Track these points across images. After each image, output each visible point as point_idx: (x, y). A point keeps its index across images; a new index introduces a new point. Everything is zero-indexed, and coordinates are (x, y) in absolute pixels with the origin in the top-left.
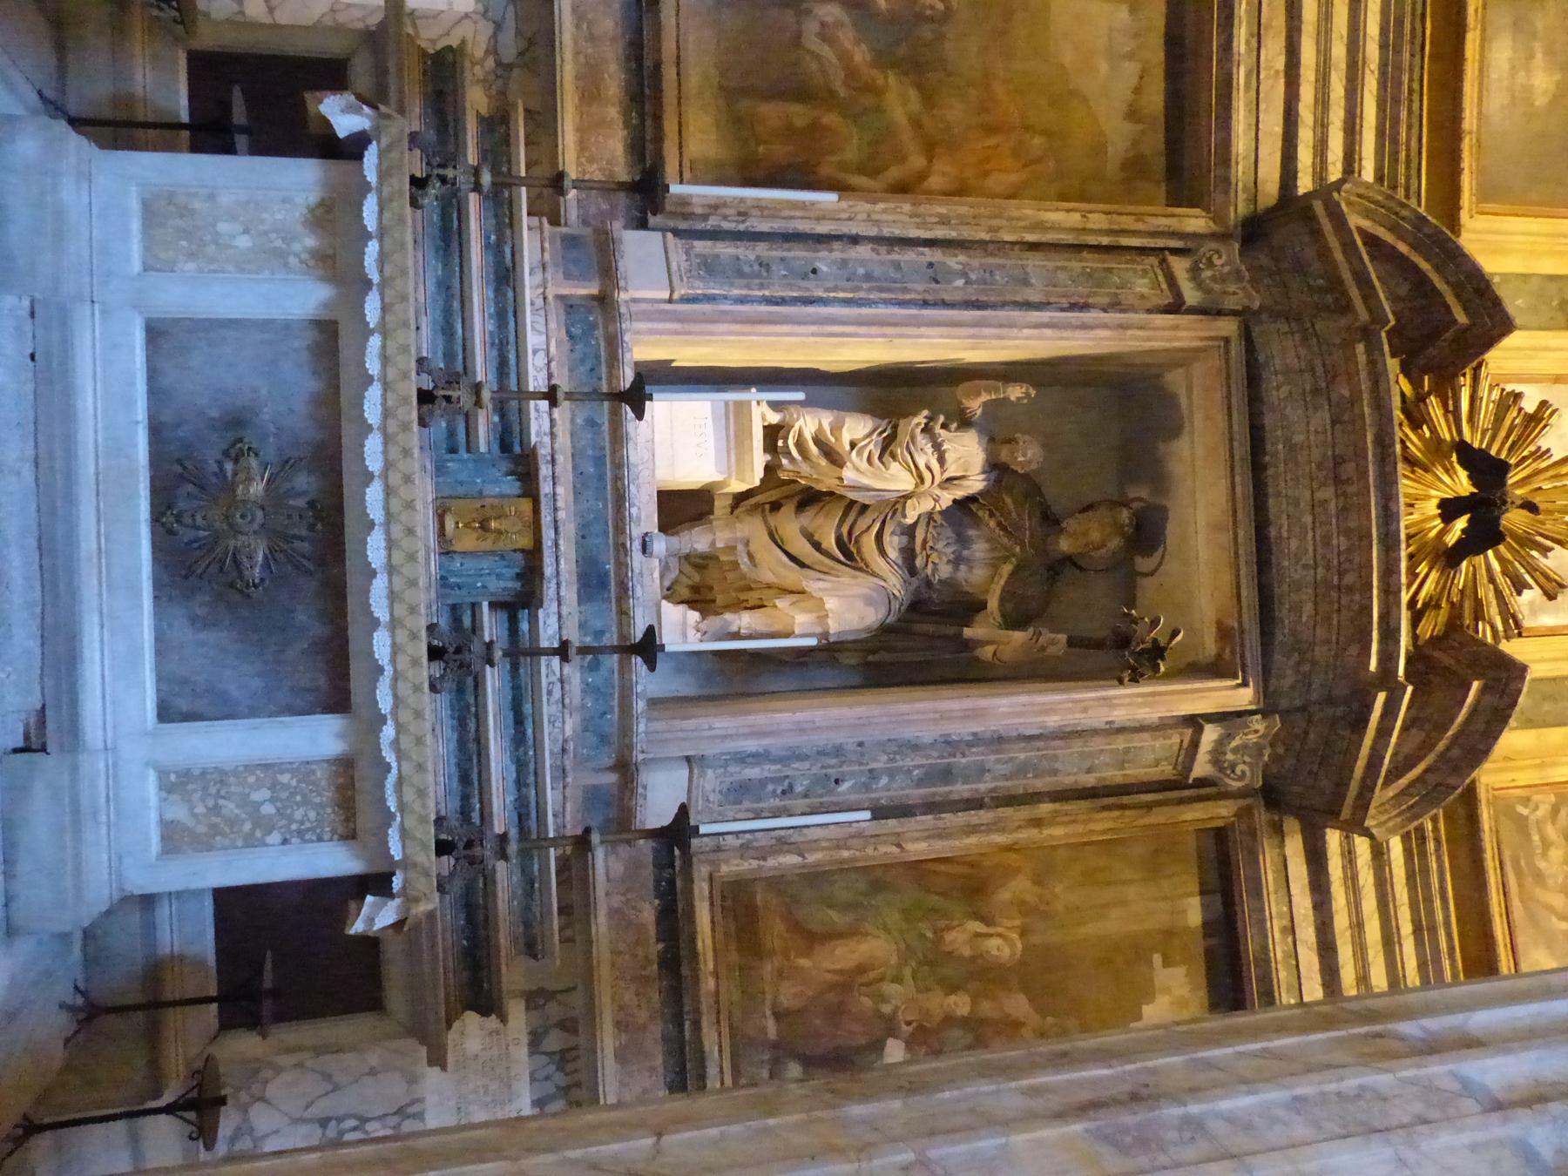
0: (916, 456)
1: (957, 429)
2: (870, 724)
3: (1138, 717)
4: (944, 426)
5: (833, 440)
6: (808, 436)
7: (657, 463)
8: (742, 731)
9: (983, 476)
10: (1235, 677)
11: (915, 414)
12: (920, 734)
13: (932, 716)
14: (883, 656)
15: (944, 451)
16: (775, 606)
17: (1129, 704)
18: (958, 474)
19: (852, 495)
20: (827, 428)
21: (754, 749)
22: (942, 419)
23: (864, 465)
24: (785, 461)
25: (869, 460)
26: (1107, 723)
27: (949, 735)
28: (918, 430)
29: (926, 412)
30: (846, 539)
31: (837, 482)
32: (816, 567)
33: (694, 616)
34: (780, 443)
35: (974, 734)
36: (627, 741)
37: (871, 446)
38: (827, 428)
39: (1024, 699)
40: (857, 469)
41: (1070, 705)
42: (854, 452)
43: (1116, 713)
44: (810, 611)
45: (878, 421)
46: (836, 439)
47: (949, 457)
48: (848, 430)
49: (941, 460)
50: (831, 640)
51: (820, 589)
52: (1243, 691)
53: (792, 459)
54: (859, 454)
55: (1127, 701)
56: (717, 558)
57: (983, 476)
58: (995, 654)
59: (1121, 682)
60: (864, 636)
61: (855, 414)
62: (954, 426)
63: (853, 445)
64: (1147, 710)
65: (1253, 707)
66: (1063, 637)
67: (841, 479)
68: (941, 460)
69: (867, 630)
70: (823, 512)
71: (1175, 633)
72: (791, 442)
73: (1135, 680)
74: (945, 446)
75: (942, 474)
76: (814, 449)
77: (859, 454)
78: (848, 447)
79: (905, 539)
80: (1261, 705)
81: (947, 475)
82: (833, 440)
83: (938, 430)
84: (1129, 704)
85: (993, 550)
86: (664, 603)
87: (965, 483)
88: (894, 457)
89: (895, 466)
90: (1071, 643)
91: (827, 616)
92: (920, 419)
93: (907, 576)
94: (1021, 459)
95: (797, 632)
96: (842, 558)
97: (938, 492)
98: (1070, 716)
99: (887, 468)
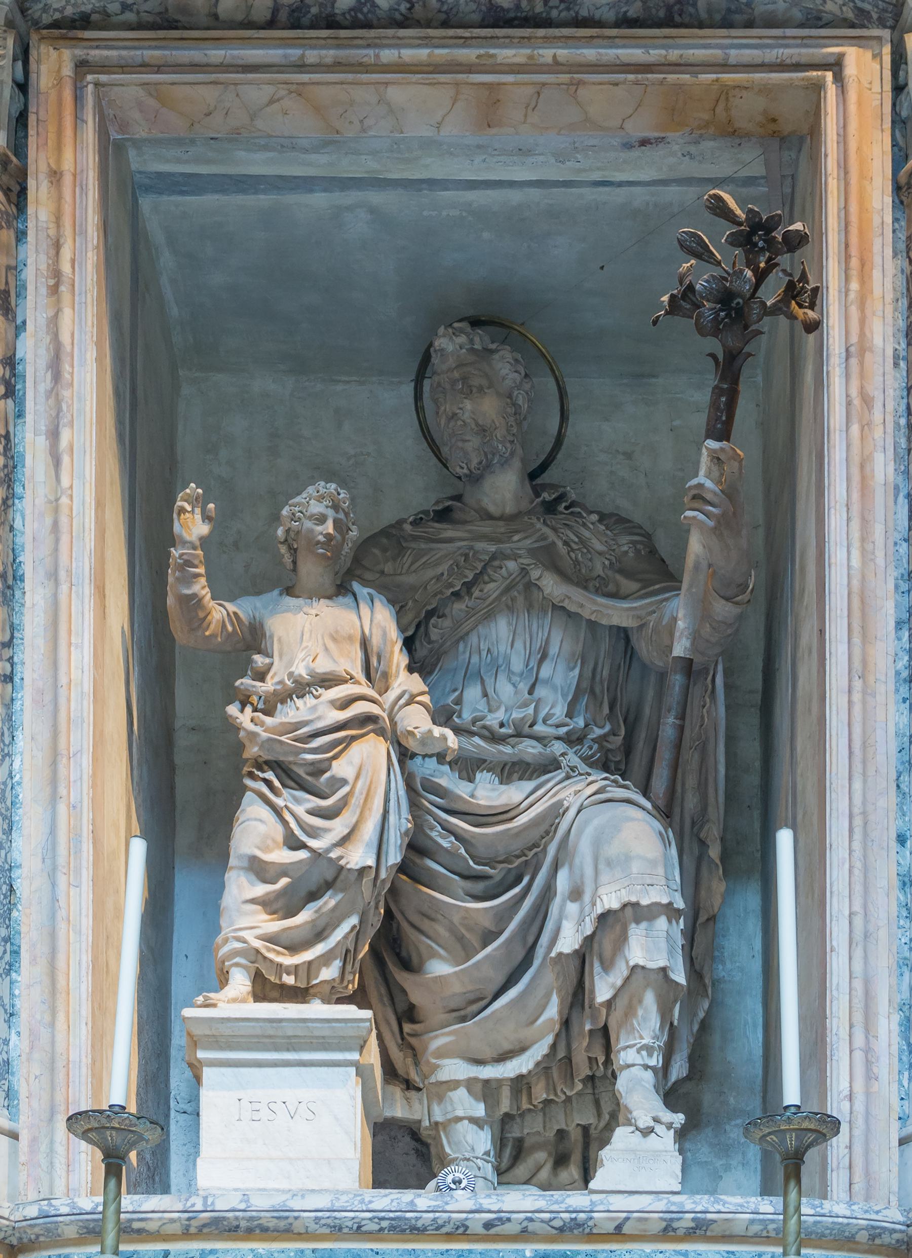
0: (320, 725)
1: (269, 655)
2: (864, 813)
3: (889, 297)
4: (261, 676)
5: (284, 881)
6: (275, 926)
7: (326, 1185)
8: (859, 1040)
9: (365, 610)
10: (818, 88)
11: (237, 729)
12: (892, 729)
13: (857, 697)
14: (713, 832)
15: (312, 674)
16: (609, 1004)
17: (862, 307)
18: (359, 655)
19: (394, 857)
20: (261, 889)
21: (895, 1028)
22: (245, 682)
23: (339, 827)
24: (329, 973)
25: (329, 814)
26: (896, 365)
27: (898, 673)
28: (268, 720)
29: (233, 710)
30: (479, 887)
31: (367, 880)
32: (531, 940)
33: (621, 1135)
34: (289, 980)
35: (899, 625)
36: (863, 1237)
37: (300, 810)
38: (261, 889)
39: (836, 521)
40: (344, 841)
41: (855, 429)
42: (313, 843)
43: (878, 341)
44: (623, 939)
45: (249, 794)
46: (285, 874)
47: (323, 666)
48: (267, 849)
49: (328, 681)
50: (680, 904)
51: (581, 921)
52: (850, 69)
53: (325, 959)
54: (313, 833)
55: (854, 311)
56: (507, 1118)
57: (365, 610)
58: (727, 599)
59: (813, 327)
60: (674, 851)
61: (233, 844)
62: (259, 660)
63: (294, 844)
64: (877, 274)
65: (887, 50)
66: (712, 444)
67: (363, 871)
68: (328, 681)
69: (666, 843)
70: (426, 925)
71: (719, 208)
72: (288, 960)
73: (815, 298)
74: (301, 670)
75: (357, 682)
76: (304, 916)
77: (313, 833)
78: (303, 855)
79: (483, 777)
80: (886, 34)
81: (360, 676)
82: (284, 881)
83: (269, 686)
84: (862, 307)
85: (511, 609)
86: (592, 1185)
87: (376, 642)
88: (318, 770)
89: (342, 768)
90: (724, 434)
91: (636, 905)
92: (245, 718)
93: (559, 774)
94: (329, 527)
95: (662, 963)
96: (516, 890)
97: (391, 695)
98: (878, 433)
99: (344, 782)
